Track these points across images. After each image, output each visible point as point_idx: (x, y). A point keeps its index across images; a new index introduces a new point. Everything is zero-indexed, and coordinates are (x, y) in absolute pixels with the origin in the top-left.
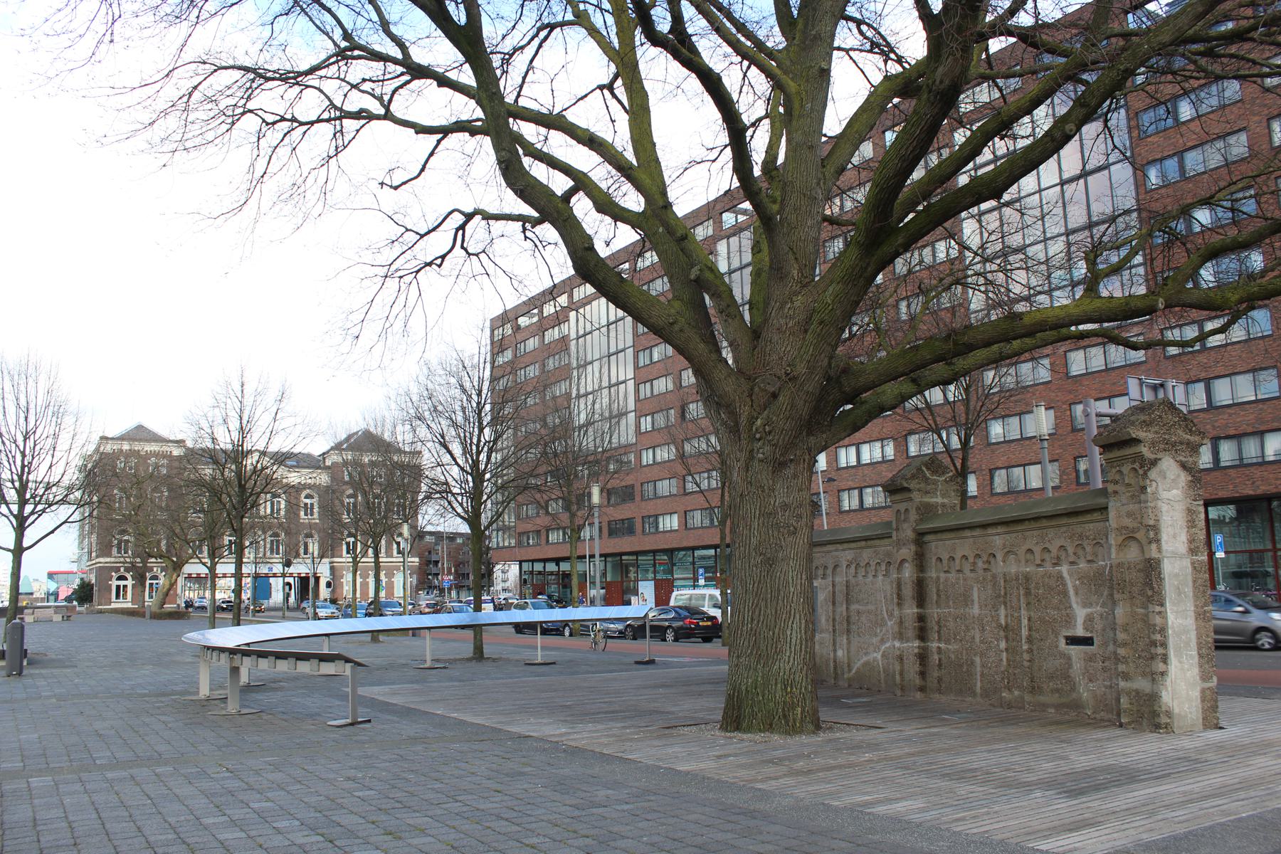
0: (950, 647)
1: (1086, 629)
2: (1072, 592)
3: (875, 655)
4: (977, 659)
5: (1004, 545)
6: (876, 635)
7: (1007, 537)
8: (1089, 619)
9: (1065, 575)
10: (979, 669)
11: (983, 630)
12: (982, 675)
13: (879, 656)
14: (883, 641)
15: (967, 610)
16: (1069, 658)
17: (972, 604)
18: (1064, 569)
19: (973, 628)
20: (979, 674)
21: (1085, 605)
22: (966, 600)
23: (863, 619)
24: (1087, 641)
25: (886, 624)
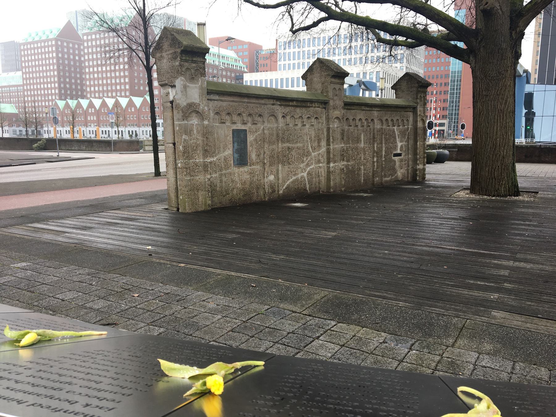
0: (349, 163)
1: (401, 150)
2: (397, 137)
3: (302, 174)
4: (362, 167)
5: (378, 116)
6: (303, 162)
7: (379, 112)
8: (402, 147)
9: (395, 130)
10: (363, 171)
11: (365, 154)
12: (364, 174)
13: (305, 174)
14: (308, 165)
15: (358, 145)
16: (395, 162)
17: (361, 142)
18: (395, 128)
19: (361, 153)
20: (363, 174)
21: (401, 141)
22: (358, 140)
23: (293, 153)
24: (400, 155)
25: (310, 155)
